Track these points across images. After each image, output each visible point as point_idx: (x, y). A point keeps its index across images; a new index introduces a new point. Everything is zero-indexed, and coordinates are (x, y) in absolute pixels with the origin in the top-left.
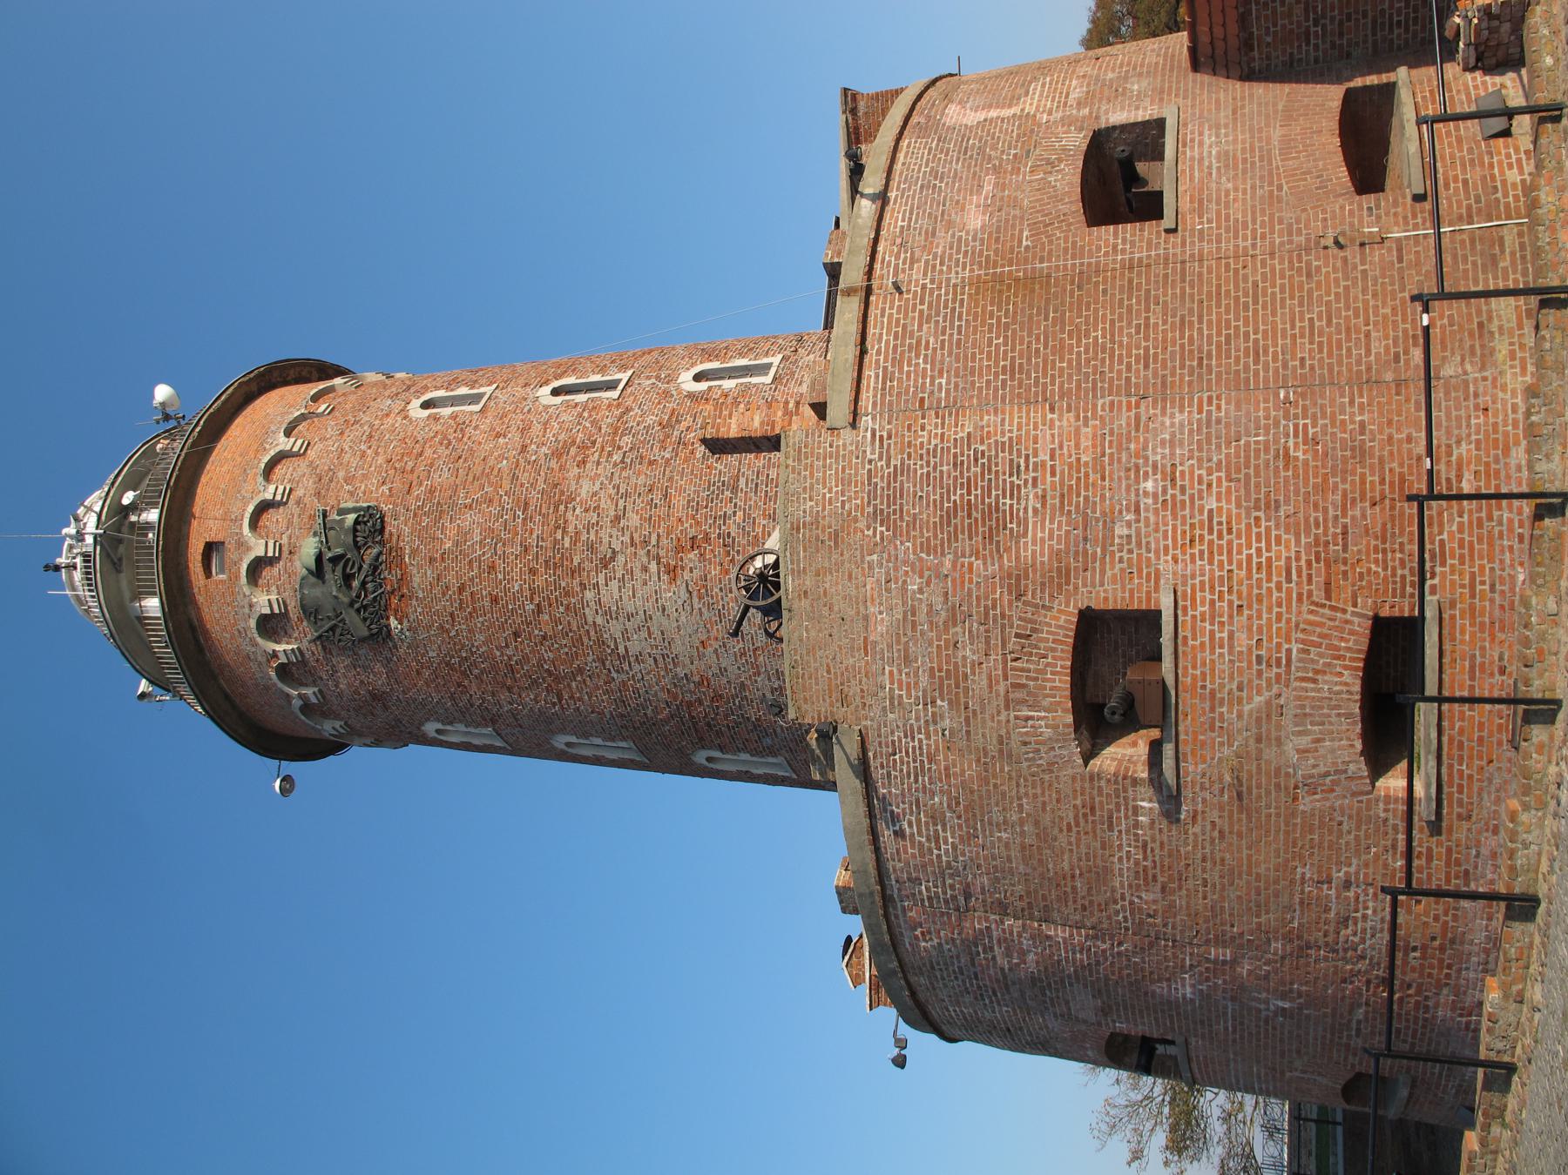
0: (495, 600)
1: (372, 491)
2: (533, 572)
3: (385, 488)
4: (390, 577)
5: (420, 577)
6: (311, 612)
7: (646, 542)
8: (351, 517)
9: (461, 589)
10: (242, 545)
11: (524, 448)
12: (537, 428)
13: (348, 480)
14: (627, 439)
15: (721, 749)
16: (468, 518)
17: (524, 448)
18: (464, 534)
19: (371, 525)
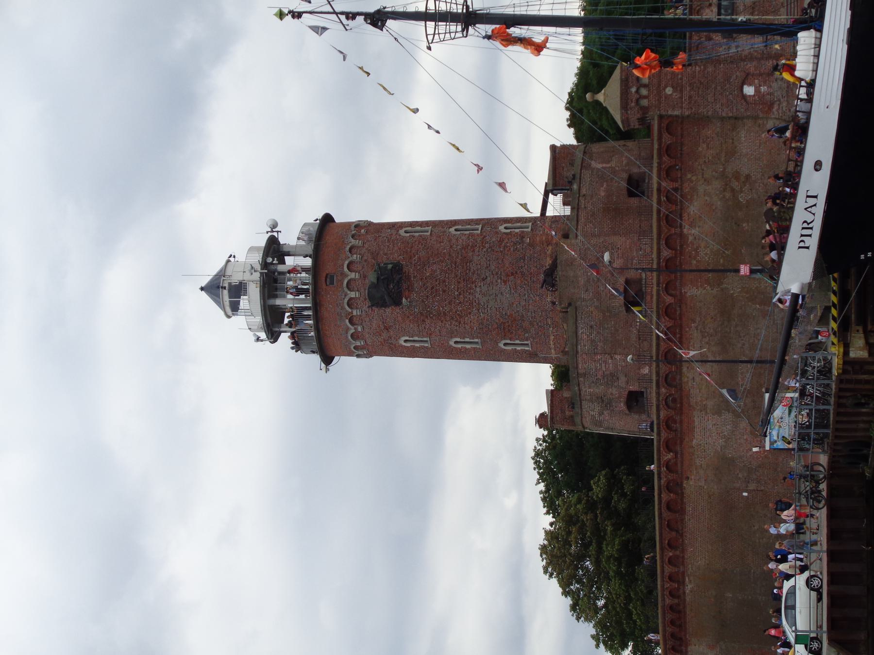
0: (444, 291)
1: (397, 257)
2: (459, 282)
3: (401, 257)
4: (405, 286)
5: (417, 285)
6: (371, 297)
7: (497, 274)
8: (390, 266)
9: (432, 288)
10: (344, 275)
11: (451, 247)
12: (454, 241)
13: (385, 254)
14: (487, 245)
15: (510, 340)
16: (435, 267)
17: (451, 247)
18: (434, 271)
19: (397, 268)
